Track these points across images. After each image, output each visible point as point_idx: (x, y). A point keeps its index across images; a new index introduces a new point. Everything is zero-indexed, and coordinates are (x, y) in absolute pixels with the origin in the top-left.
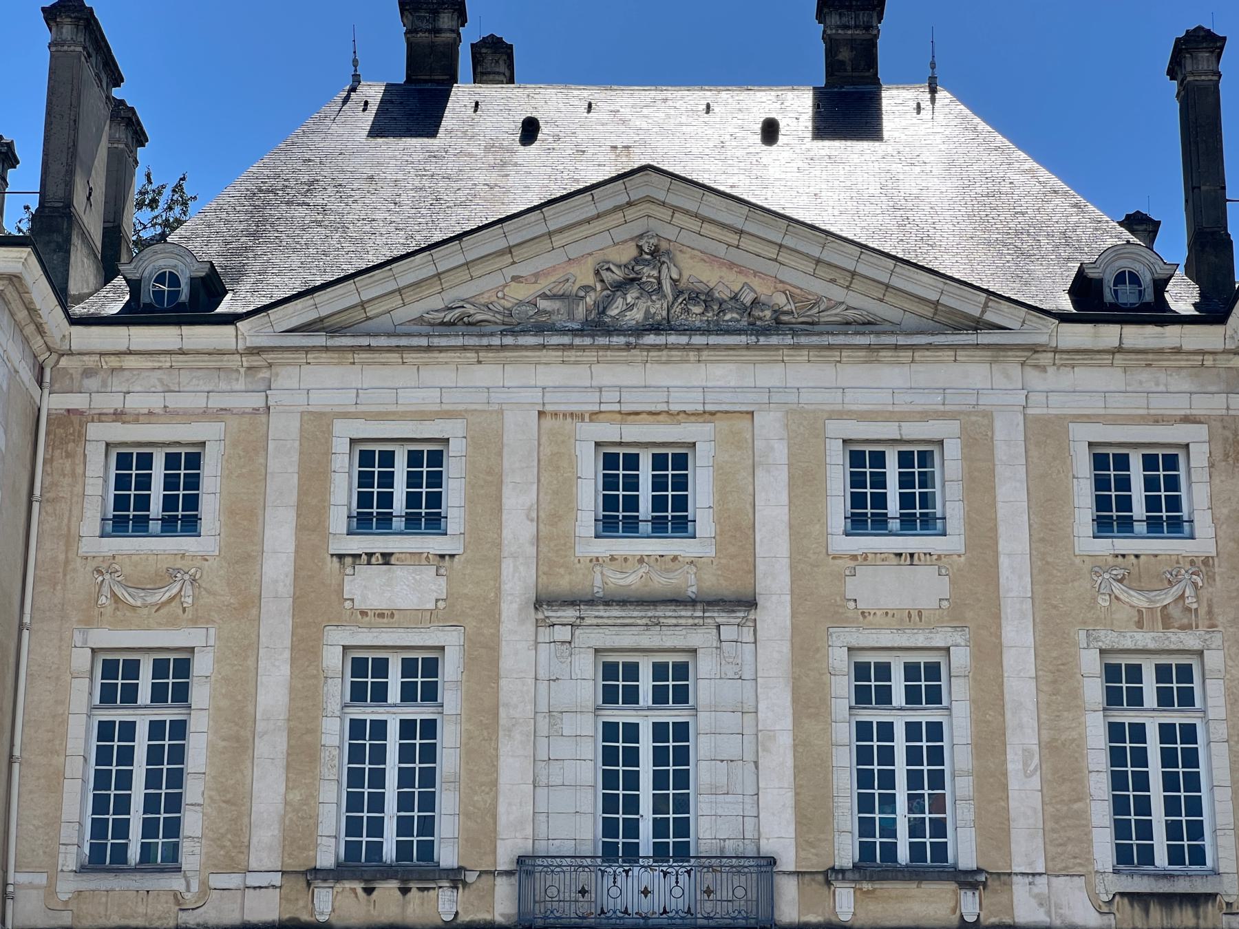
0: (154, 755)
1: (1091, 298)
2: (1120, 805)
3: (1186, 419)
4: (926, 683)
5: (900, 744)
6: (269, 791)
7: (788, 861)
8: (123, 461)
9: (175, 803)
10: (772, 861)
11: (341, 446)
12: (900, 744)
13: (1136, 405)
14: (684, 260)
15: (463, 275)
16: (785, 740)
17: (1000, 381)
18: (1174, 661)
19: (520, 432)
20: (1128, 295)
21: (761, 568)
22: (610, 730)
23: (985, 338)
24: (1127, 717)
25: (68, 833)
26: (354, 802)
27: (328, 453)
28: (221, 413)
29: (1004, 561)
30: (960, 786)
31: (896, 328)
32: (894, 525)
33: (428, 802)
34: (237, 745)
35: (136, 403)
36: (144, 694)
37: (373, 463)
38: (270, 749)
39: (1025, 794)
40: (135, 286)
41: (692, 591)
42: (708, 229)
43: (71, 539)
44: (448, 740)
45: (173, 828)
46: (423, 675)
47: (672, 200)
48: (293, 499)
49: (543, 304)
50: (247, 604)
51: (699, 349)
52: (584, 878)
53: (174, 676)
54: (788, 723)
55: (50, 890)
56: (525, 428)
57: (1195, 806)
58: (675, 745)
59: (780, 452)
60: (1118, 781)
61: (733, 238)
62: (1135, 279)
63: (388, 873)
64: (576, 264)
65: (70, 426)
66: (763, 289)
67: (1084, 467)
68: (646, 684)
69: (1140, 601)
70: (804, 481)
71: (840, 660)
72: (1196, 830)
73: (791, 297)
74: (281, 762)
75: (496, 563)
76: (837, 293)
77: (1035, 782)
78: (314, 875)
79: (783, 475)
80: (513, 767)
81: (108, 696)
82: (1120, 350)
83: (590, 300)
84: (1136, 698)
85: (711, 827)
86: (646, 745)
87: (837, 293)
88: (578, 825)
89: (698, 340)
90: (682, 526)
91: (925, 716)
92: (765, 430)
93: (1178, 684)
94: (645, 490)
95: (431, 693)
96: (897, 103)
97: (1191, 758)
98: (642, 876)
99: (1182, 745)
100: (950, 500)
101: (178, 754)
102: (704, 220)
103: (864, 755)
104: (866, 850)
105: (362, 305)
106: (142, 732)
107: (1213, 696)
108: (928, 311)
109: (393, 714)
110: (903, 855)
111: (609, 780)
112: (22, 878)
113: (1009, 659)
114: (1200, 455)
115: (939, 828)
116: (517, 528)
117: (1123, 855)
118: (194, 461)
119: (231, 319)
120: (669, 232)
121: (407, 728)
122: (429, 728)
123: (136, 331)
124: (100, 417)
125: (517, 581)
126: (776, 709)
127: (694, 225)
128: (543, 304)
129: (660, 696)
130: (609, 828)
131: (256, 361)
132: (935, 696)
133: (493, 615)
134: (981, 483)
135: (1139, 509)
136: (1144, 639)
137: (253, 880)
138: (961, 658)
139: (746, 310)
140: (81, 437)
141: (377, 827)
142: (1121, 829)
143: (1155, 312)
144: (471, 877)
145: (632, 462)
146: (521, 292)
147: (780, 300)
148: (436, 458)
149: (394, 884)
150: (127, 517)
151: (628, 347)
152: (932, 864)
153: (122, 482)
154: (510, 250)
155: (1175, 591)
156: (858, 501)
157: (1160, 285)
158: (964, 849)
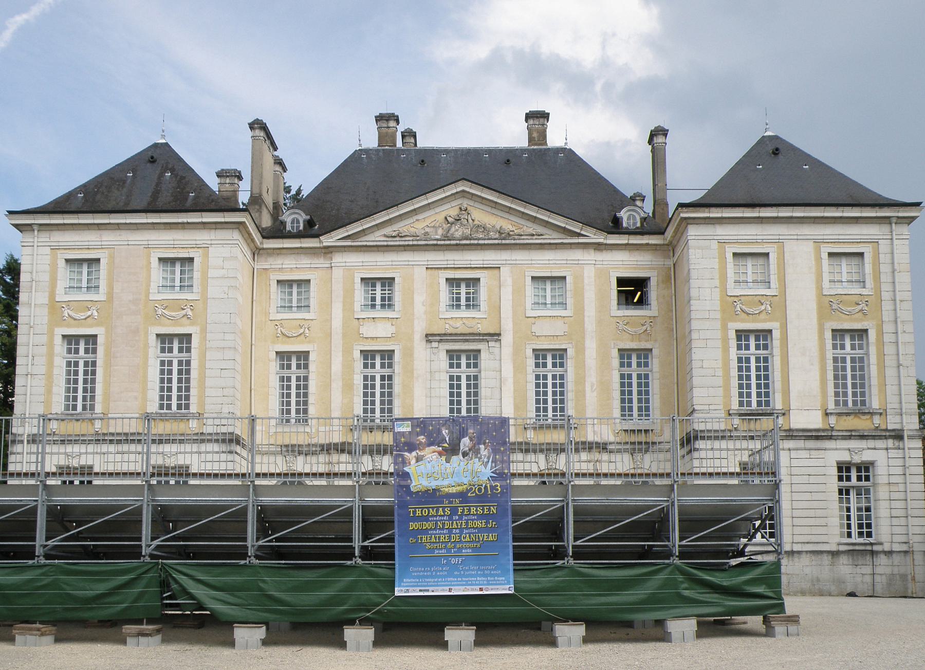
5: (550, 382)
12: (550, 382)
30: (570, 396)
54: (511, 375)
57: (647, 401)
77: (595, 394)
85: (487, 409)
97: (647, 385)
99: (644, 380)
103: (538, 385)
107: (655, 363)
111: (451, 395)
122: (390, 378)
133: (411, 339)
155: (644, 328)
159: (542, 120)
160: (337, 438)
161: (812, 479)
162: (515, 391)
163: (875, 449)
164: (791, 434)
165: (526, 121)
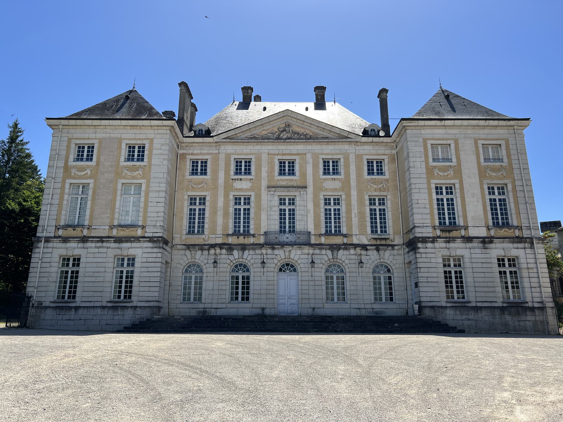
0: (199, 214)
1: (366, 133)
2: (372, 223)
3: (384, 155)
4: (337, 201)
5: (332, 212)
6: (220, 220)
7: (313, 233)
8: (193, 162)
9: (203, 223)
10: (310, 233)
11: (232, 160)
12: (332, 212)
13: (375, 152)
14: (294, 127)
15: (254, 129)
16: (312, 211)
17: (350, 148)
18: (381, 197)
19: (264, 157)
20: (373, 133)
21: (308, 181)
22: (281, 210)
23: (348, 140)
24: (373, 207)
25: (184, 228)
26: (235, 223)
27: (230, 161)
28: (211, 154)
29: (351, 180)
30: (343, 219)
31: (332, 139)
32: (331, 174)
33: (248, 222)
34: (214, 212)
35: (196, 152)
36: (198, 204)
37: (238, 163)
38: (220, 213)
39: (355, 221)
40: (195, 132)
41: (295, 185)
42: (298, 121)
43: (184, 176)
44: (252, 211)
45: (203, 227)
46: (247, 200)
47: (291, 115)
48: (224, 169)
49: (269, 135)
50: (216, 188)
51: (296, 142)
52: (276, 236)
53: (203, 200)
55: (181, 238)
56: (266, 156)
57: (385, 223)
58: (292, 213)
59: (311, 161)
60: (371, 219)
61: (302, 123)
62: (374, 130)
63: (241, 235)
64: (275, 127)
65: (184, 156)
66: (308, 132)
67: (366, 163)
68: (287, 202)
69: (375, 187)
70: (315, 166)
71: (322, 197)
72: (385, 227)
73: (313, 133)
74: (222, 215)
75: (260, 180)
76: (321, 132)
77: (357, 219)
78: (228, 235)
79: (311, 165)
80: (264, 217)
81: (191, 204)
82: (372, 142)
83: (277, 134)
84: (375, 204)
85: (299, 226)
86: (287, 212)
87: (321, 132)
88: (275, 226)
89: (296, 141)
90: (293, 174)
91: (337, 207)
92: (308, 157)
93: (382, 202)
94: (287, 168)
95: (249, 203)
96: (328, 105)
97: (384, 214)
98: (287, 235)
99: (383, 212)
100: (341, 169)
101: (204, 214)
102: (297, 119)
103: (326, 214)
104: (326, 231)
105: (236, 134)
106: (197, 210)
108: (338, 135)
109: (242, 207)
110: (333, 232)
111: (281, 219)
112: (176, 236)
113: (352, 197)
114: (386, 161)
115: (339, 227)
116: (264, 174)
117: (372, 231)
118: (206, 162)
119: (212, 137)
120: (291, 122)
121: (245, 209)
122: (249, 209)
123: (195, 139)
124: (189, 154)
125: (264, 183)
126: (310, 206)
127: (295, 120)
128: (269, 135)
129: (290, 204)
130: (281, 227)
131: (217, 144)
132: (339, 204)
134: (347, 166)
135: (375, 171)
136: (376, 193)
137: (217, 236)
138: (343, 197)
139: (305, 136)
140: (185, 158)
141: (239, 227)
142: (372, 227)
143: (378, 136)
144: (256, 236)
145: (284, 163)
146: (264, 132)
147: (311, 134)
148: (250, 162)
149: (242, 237)
150: (194, 172)
151: (284, 142)
152: (338, 233)
153: (193, 166)
154: (262, 125)
156: (325, 169)
157: (379, 131)
158: (344, 230)
159: (322, 91)
160: (219, 241)
161: (484, 265)
162: (314, 217)
163: (517, 248)
164: (469, 239)
165: (315, 91)
